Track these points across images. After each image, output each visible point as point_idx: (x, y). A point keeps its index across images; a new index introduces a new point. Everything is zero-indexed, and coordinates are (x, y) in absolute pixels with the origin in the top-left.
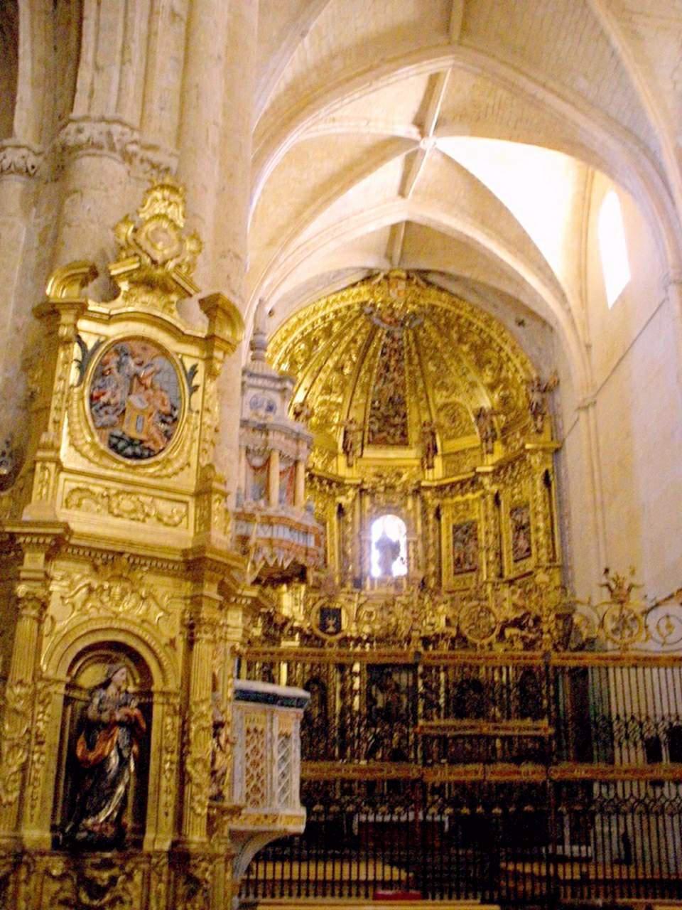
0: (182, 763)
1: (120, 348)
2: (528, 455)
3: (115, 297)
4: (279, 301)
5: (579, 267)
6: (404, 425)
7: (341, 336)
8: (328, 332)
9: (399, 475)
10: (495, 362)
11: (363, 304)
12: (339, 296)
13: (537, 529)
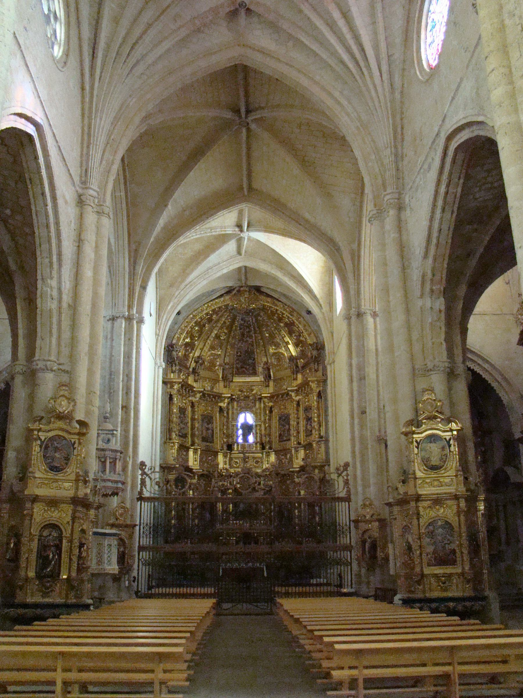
0: (70, 556)
1: (52, 439)
2: (310, 383)
3: (50, 423)
4: (182, 308)
5: (329, 290)
7: (217, 321)
8: (210, 320)
9: (252, 390)
11: (227, 306)
12: (214, 302)
13: (314, 421)
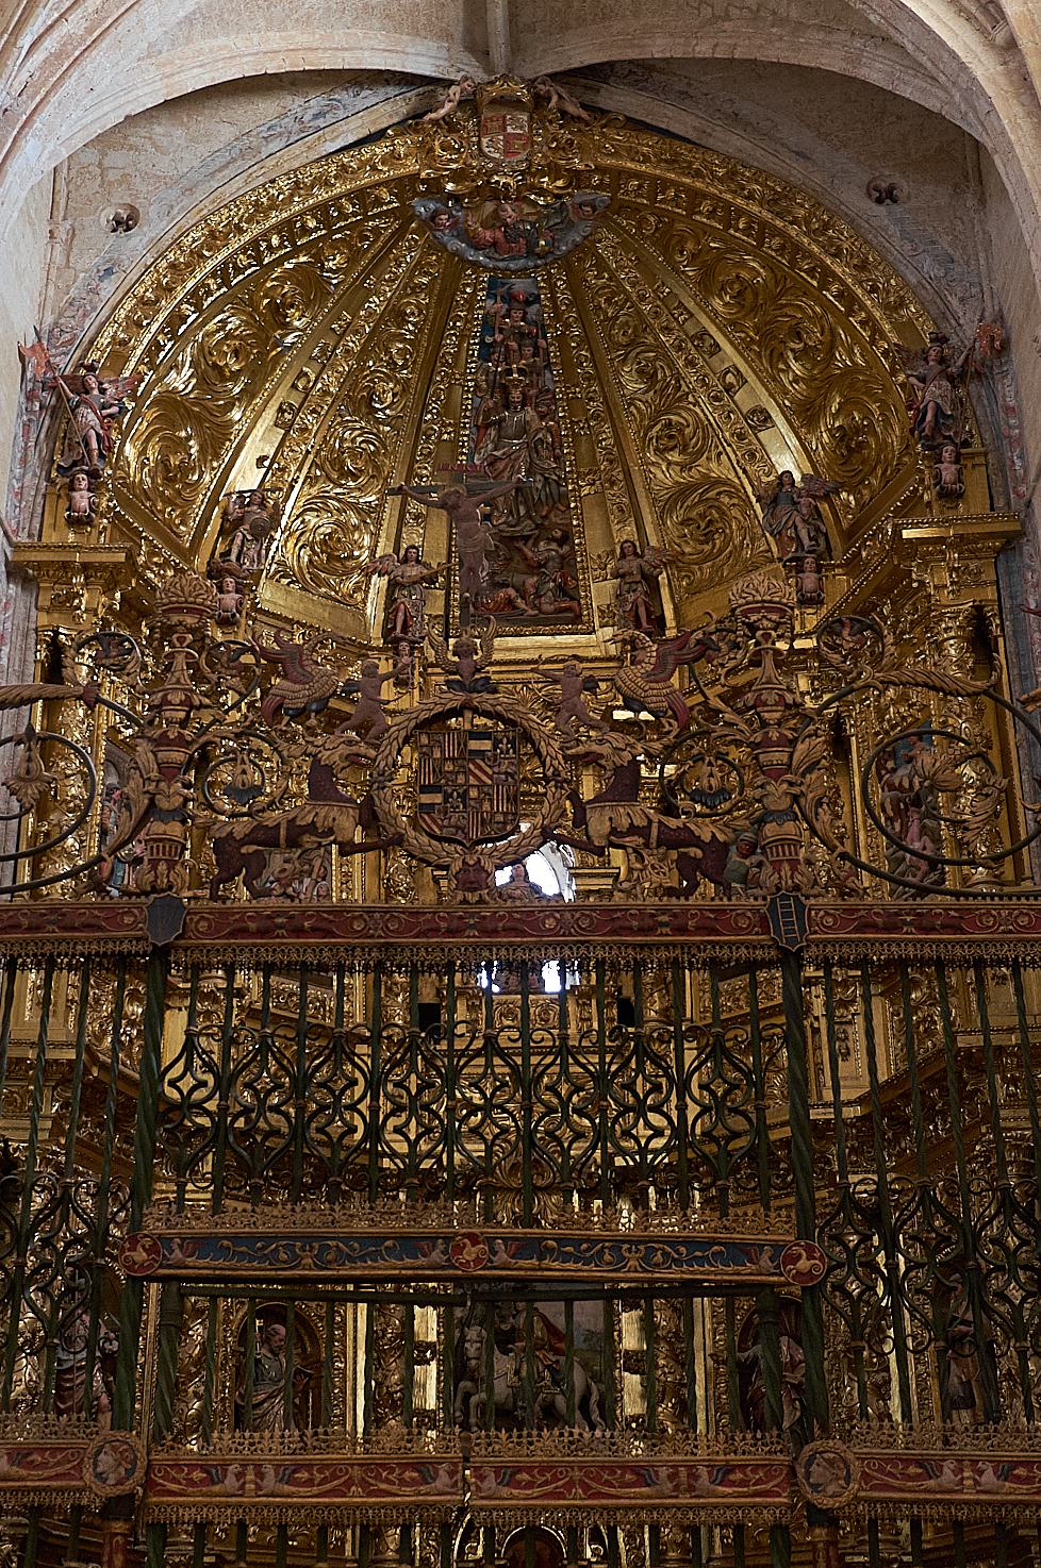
6: (567, 563)
7: (356, 295)
8: (311, 285)
10: (815, 336)
11: (405, 186)
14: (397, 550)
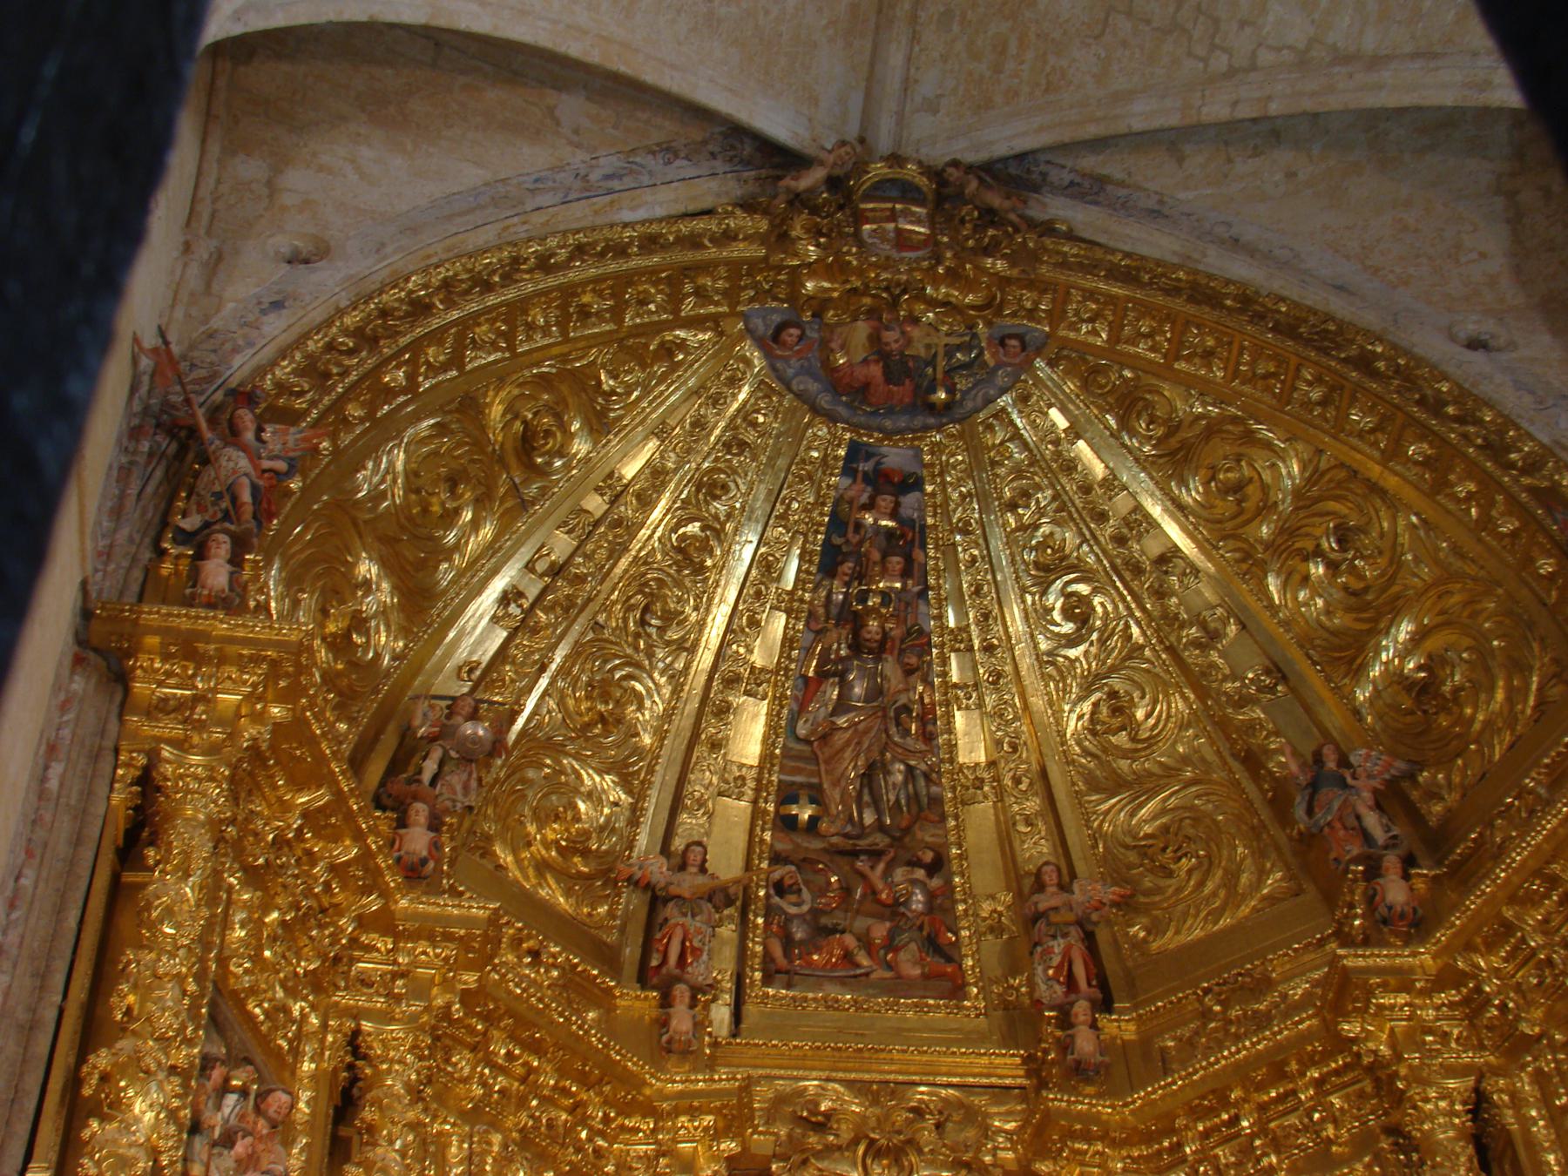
14: (665, 850)
